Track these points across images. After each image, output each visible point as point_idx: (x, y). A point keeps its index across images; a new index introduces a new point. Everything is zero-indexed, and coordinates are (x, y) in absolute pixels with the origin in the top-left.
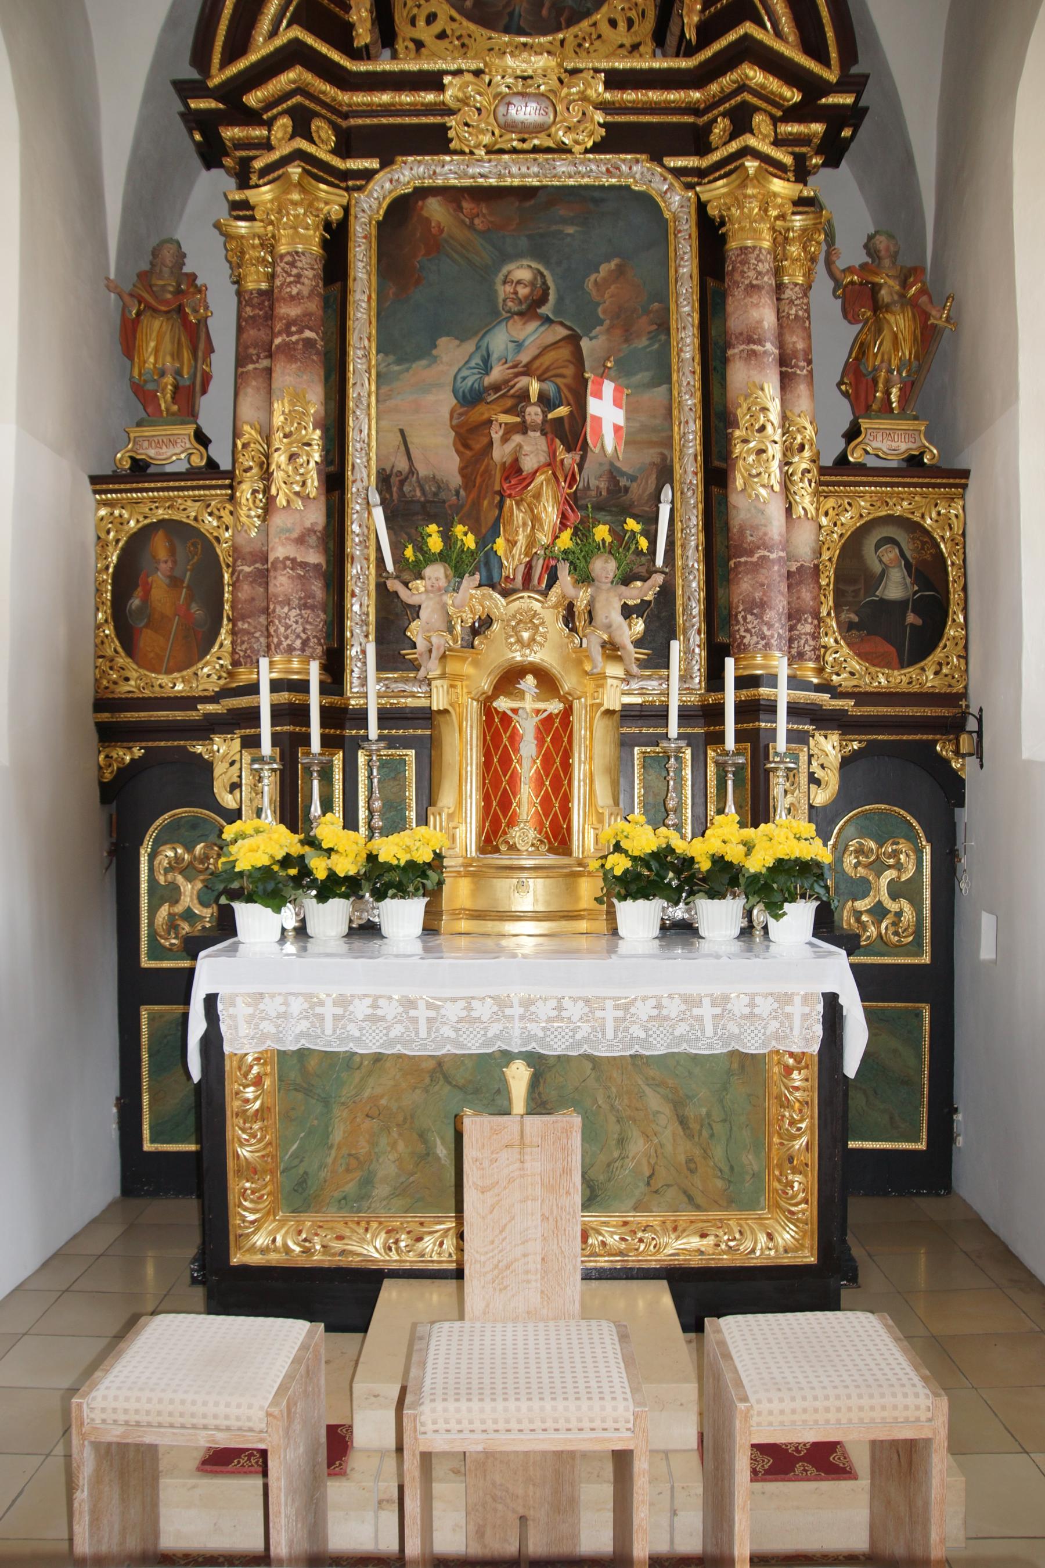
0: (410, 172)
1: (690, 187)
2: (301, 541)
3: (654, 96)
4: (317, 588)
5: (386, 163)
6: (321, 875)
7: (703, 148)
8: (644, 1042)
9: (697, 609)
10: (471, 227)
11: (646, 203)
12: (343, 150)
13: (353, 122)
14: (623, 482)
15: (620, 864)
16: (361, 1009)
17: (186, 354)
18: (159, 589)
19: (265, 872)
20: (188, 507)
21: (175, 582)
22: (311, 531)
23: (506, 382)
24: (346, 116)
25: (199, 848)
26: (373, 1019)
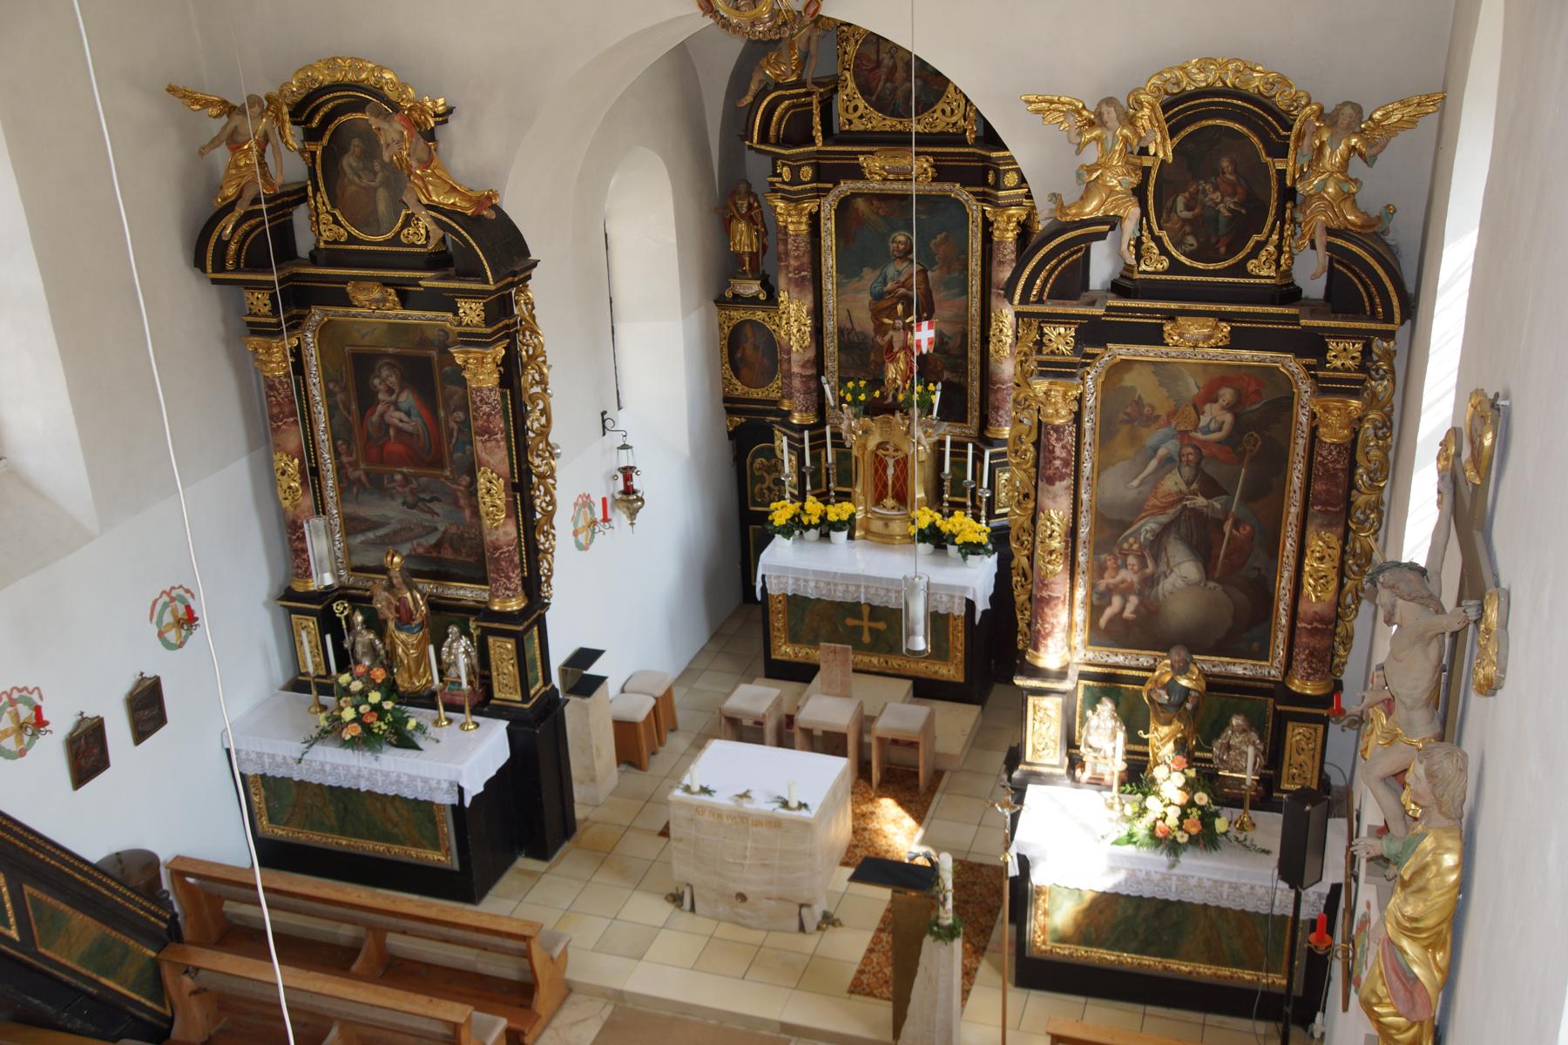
2: (803, 366)
5: (836, 184)
7: (985, 183)
9: (977, 400)
11: (960, 206)
12: (814, 179)
15: (913, 530)
16: (812, 584)
20: (759, 315)
21: (756, 348)
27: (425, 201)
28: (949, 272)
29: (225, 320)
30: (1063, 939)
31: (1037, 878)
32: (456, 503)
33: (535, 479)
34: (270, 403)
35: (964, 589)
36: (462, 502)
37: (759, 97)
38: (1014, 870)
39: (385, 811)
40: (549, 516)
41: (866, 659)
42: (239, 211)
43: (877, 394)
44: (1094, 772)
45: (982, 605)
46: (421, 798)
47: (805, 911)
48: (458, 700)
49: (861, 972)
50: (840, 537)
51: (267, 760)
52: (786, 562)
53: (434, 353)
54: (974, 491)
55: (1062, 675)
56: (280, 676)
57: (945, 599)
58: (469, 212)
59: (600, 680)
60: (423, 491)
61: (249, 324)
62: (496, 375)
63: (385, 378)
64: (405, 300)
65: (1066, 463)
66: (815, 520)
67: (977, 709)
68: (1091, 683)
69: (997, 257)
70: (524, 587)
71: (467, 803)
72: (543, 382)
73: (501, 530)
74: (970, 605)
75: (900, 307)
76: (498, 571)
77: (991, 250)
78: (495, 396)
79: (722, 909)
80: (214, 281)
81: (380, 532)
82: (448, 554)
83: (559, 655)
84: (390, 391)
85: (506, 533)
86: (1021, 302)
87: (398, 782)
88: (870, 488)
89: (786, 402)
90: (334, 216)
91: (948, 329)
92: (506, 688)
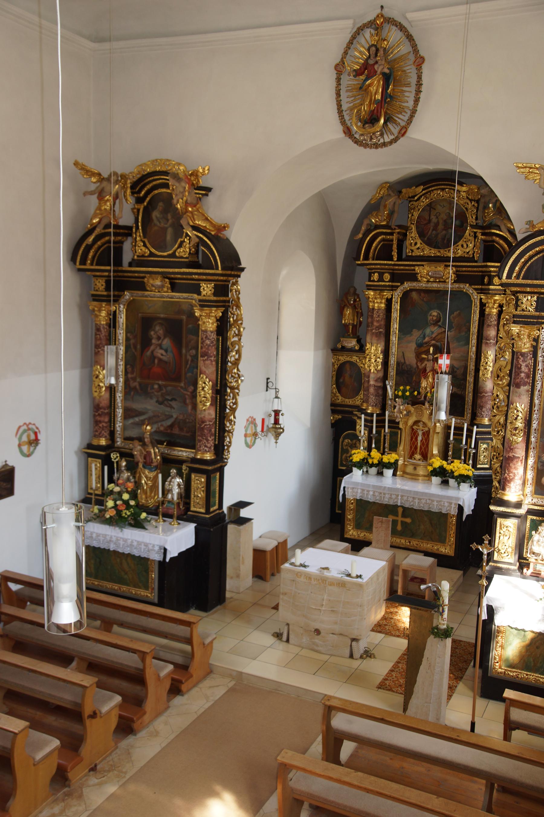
1: (478, 293)
2: (376, 381)
4: (380, 392)
5: (402, 283)
6: (370, 462)
7: (483, 284)
8: (423, 507)
9: (470, 404)
10: (423, 300)
11: (468, 297)
12: (392, 280)
13: (395, 272)
14: (455, 370)
15: (430, 469)
16: (371, 493)
17: (356, 318)
18: (347, 377)
19: (359, 462)
21: (351, 376)
22: (379, 378)
23: (429, 342)
24: (393, 270)
25: (354, 441)
26: (374, 495)
27: (191, 223)
29: (81, 296)
30: (512, 666)
31: (499, 620)
32: (184, 402)
33: (229, 391)
34: (96, 339)
35: (458, 499)
36: (188, 401)
37: (365, 235)
38: (484, 616)
40: (233, 410)
41: (398, 540)
42: (97, 231)
43: (416, 393)
44: (535, 569)
45: (468, 511)
46: (142, 556)
47: (354, 643)
48: (170, 512)
49: (385, 679)
50: (389, 473)
52: (357, 483)
53: (184, 317)
54: (466, 450)
55: (518, 505)
56: (77, 494)
57: (446, 504)
58: (213, 233)
59: (247, 520)
61: (93, 295)
62: (215, 324)
63: (158, 330)
64: (174, 287)
65: (528, 376)
67: (459, 573)
68: (535, 518)
69: (487, 322)
70: (215, 449)
71: (167, 560)
72: (239, 335)
73: (207, 412)
74: (461, 509)
75: (431, 349)
76: (202, 435)
77: (483, 321)
78: (214, 336)
79: (305, 640)
80: (79, 270)
81: (142, 418)
82: (176, 431)
83: (228, 501)
84: (159, 338)
85: (209, 414)
86: (507, 278)
87: (131, 545)
88: (408, 447)
89: (365, 405)
90: (144, 242)
91: (456, 364)
92: (197, 506)
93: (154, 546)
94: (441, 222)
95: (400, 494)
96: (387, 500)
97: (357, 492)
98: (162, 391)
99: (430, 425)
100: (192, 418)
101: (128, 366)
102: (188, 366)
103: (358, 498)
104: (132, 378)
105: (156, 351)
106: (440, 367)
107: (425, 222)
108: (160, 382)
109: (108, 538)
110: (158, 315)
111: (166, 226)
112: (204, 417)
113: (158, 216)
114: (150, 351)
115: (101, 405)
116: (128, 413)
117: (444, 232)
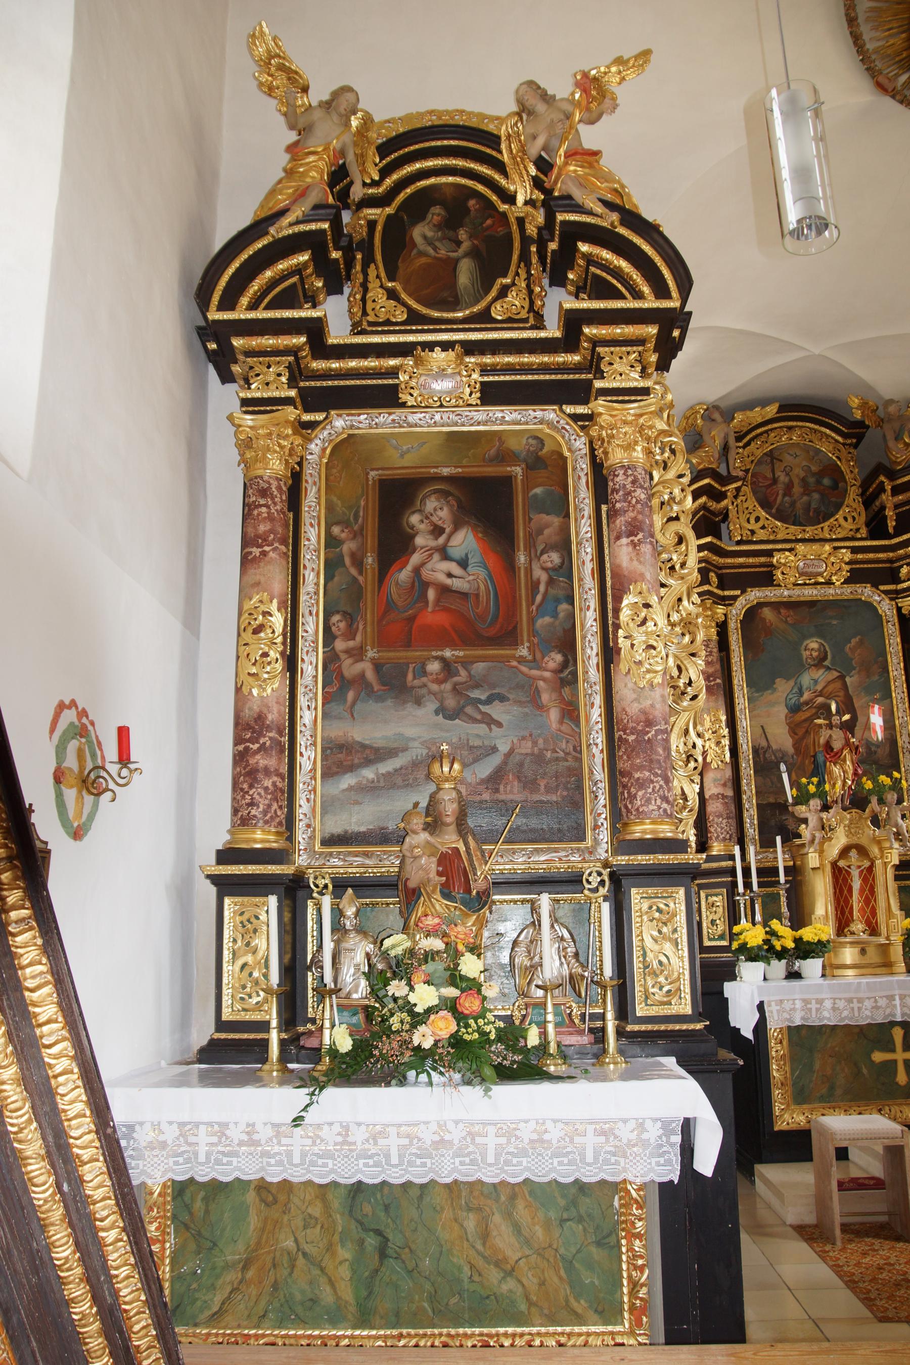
0: (755, 595)
2: (724, 785)
3: (871, 556)
5: (743, 592)
6: (778, 948)
10: (786, 622)
11: (870, 607)
12: (721, 586)
14: (873, 749)
16: (828, 1004)
19: (759, 947)
23: (811, 700)
24: (720, 568)
26: (834, 1009)
28: (868, 677)
32: (535, 700)
36: (545, 697)
39: (485, 1236)
46: (590, 1176)
51: (203, 1139)
53: (518, 471)
60: (477, 686)
66: (791, 945)
84: (437, 531)
93: (641, 1126)
94: (796, 482)
95: (897, 992)
96: (868, 1013)
97: (794, 1009)
98: (456, 679)
99: (875, 851)
100: (564, 746)
101: (336, 618)
102: (539, 598)
103: (798, 1022)
104: (348, 652)
105: (429, 566)
106: (875, 732)
107: (768, 482)
108: (448, 653)
109: (428, 1136)
110: (432, 471)
111: (453, 255)
112: (652, 706)
113: (430, 234)
114: (409, 567)
115: (270, 717)
116: (340, 757)
117: (805, 498)
